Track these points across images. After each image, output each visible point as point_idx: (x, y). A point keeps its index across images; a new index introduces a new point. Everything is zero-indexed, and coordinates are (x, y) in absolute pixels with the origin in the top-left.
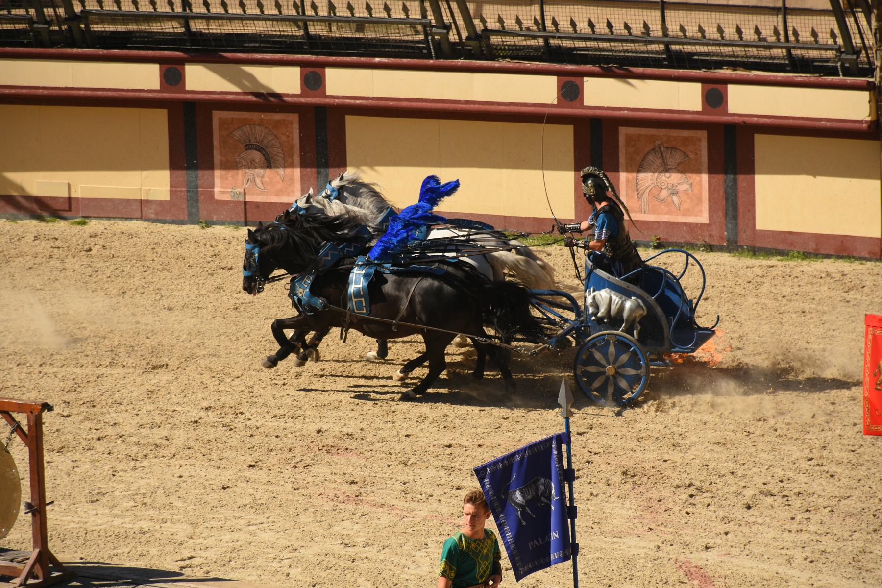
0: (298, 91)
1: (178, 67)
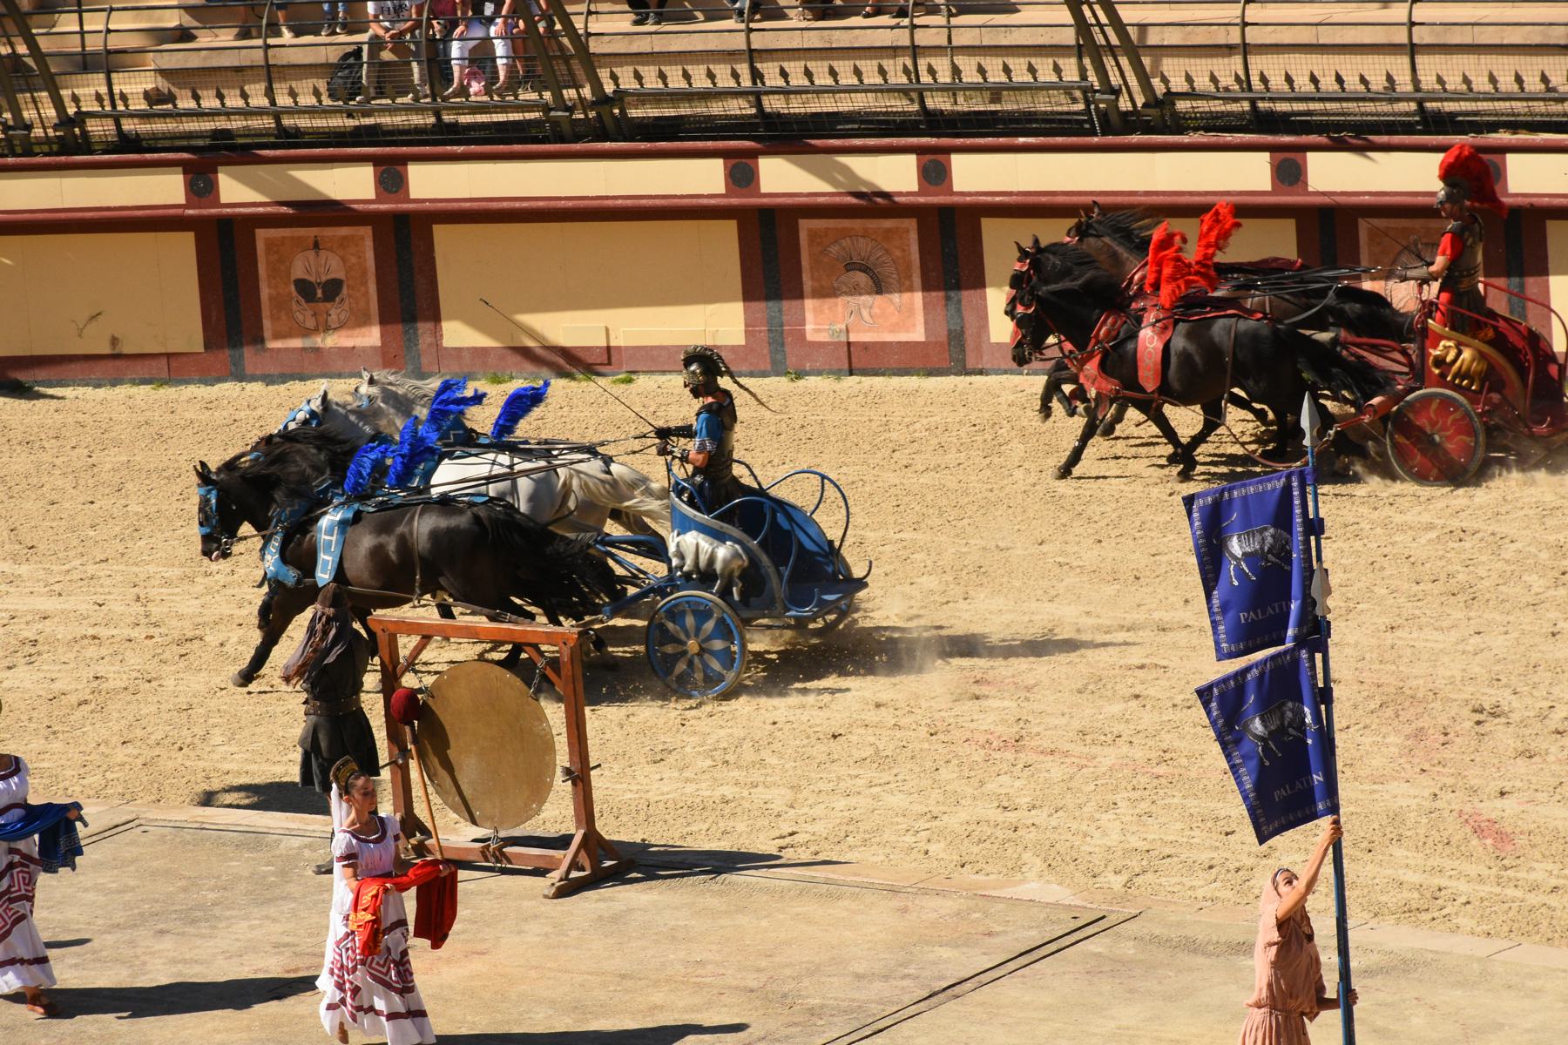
0: (371, 195)
1: (399, 168)
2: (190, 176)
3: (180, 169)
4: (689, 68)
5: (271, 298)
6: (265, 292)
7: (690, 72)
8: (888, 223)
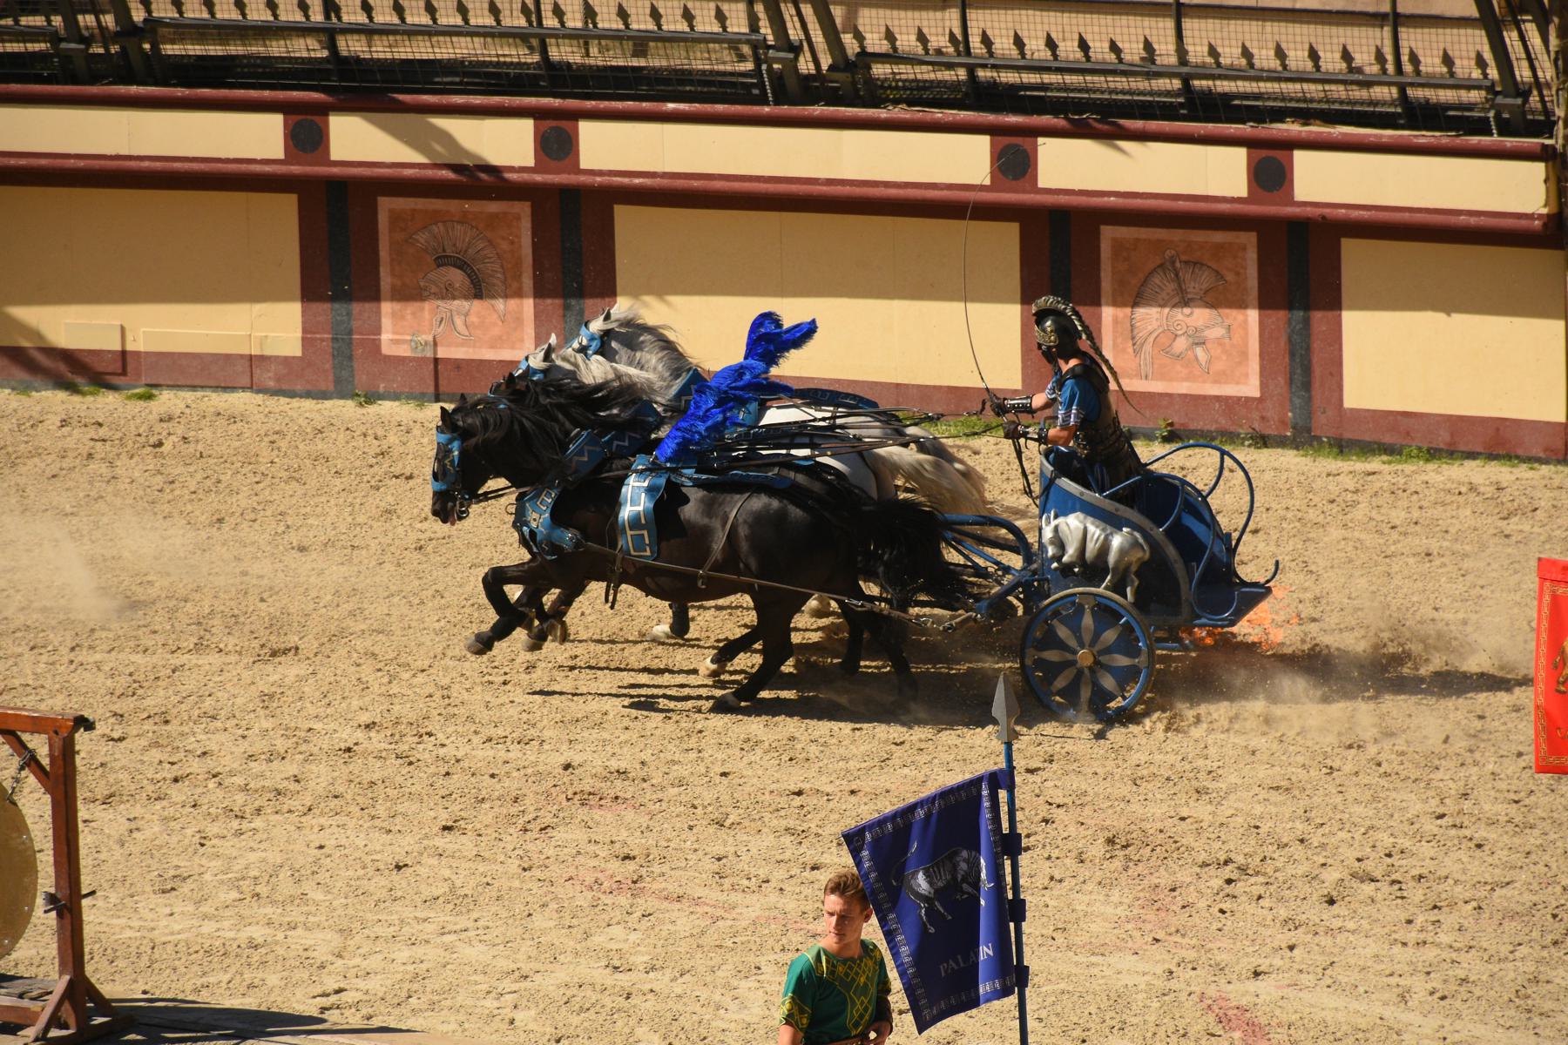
8: (494, 207)
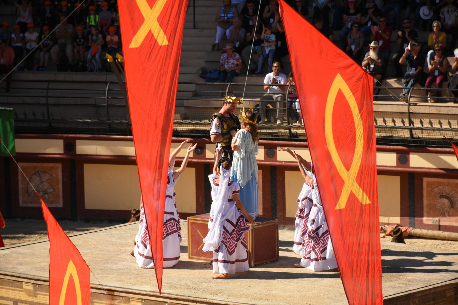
2: (399, 155)
3: (263, 147)
4: (441, 121)
5: (427, 205)
6: (425, 202)
7: (442, 122)
